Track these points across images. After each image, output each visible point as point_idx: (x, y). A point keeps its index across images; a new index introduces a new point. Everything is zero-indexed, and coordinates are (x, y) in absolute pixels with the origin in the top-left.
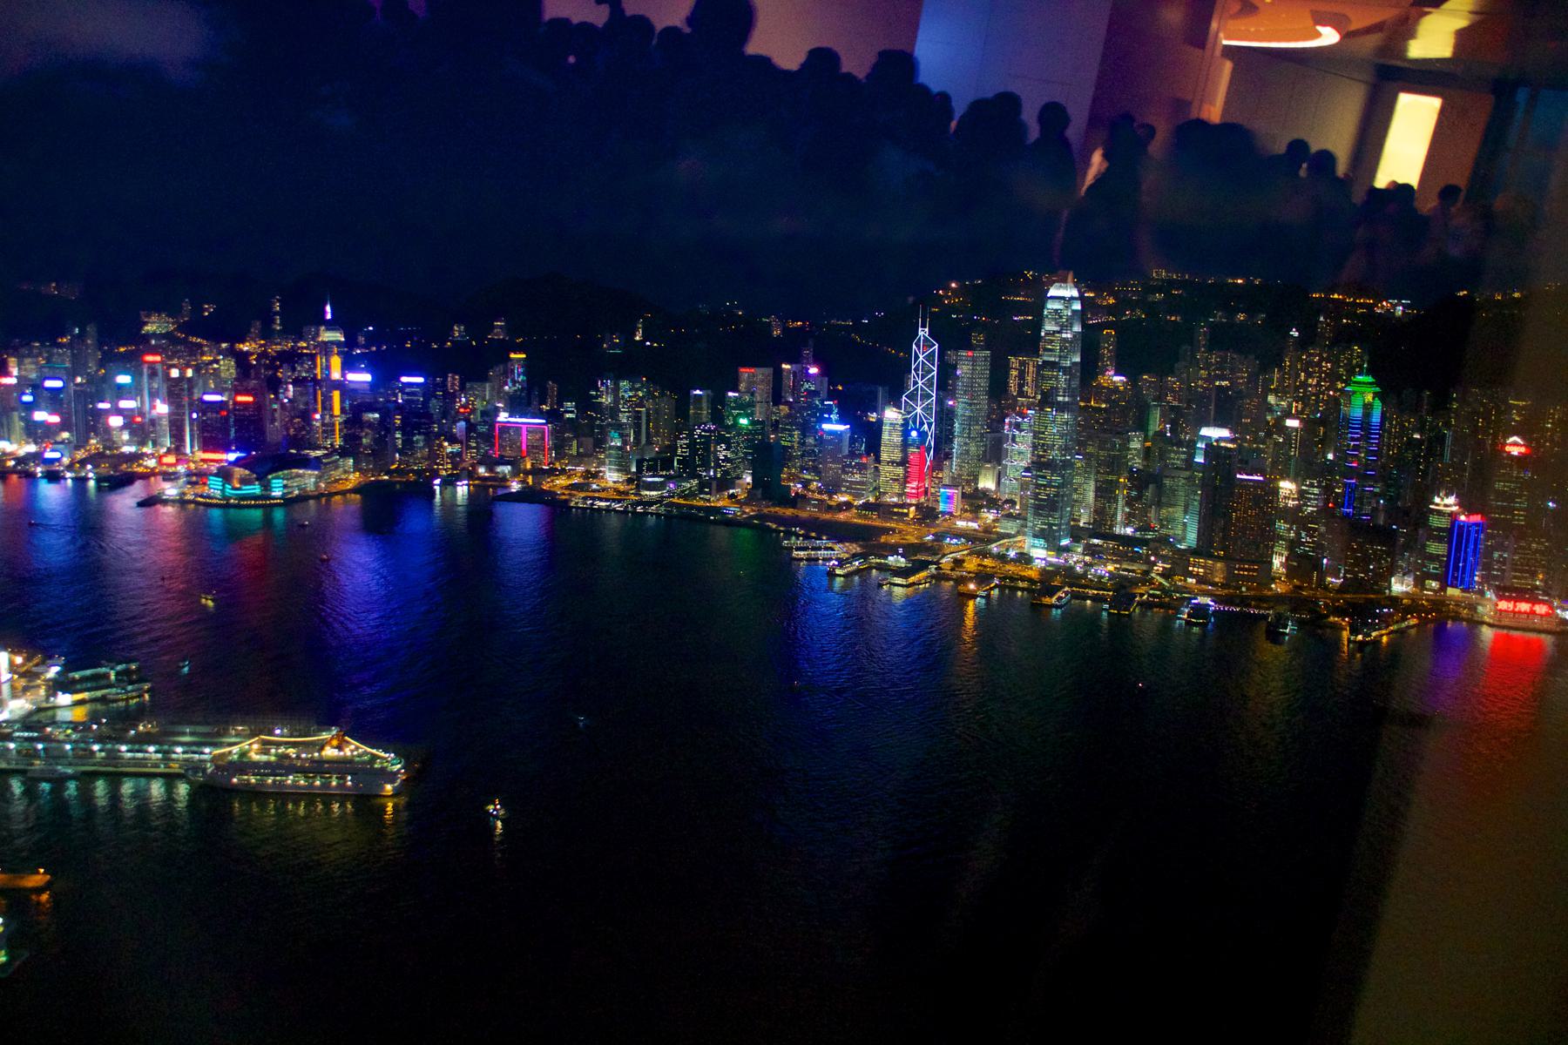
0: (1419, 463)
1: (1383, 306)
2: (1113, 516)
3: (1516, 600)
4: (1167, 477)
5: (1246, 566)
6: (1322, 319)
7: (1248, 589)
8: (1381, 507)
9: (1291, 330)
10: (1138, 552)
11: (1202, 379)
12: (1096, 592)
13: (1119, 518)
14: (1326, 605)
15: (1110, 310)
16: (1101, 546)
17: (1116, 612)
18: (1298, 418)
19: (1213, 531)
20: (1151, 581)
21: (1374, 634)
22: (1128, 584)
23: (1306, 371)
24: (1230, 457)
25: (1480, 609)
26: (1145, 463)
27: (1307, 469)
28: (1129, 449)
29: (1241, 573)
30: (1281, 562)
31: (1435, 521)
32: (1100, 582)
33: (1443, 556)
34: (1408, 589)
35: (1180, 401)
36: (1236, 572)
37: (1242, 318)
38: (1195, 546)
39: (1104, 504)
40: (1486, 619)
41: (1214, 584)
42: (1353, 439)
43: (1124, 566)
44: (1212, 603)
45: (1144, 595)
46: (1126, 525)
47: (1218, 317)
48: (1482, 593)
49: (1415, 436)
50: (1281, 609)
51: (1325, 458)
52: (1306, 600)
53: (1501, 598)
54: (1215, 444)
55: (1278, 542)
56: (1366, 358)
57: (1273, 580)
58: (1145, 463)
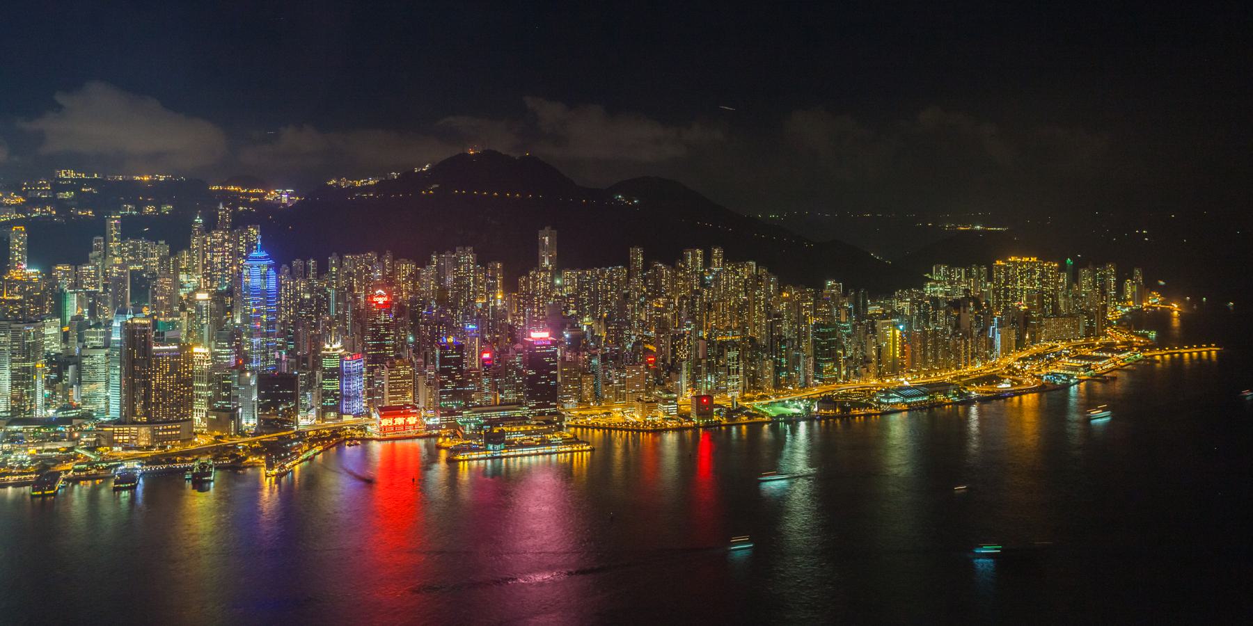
0: (312, 318)
1: (271, 195)
2: (31, 402)
3: (395, 416)
4: (87, 357)
5: (170, 427)
6: (221, 207)
7: (173, 446)
8: (284, 359)
9: (196, 218)
10: (61, 431)
11: (116, 265)
12: (17, 477)
13: (40, 400)
14: (245, 449)
15: (19, 209)
16: (21, 432)
17: (40, 493)
18: (208, 291)
19: (135, 400)
20: (75, 457)
21: (287, 465)
22: (52, 464)
23: (211, 251)
24: (145, 331)
25: (369, 428)
26: (64, 346)
27: (224, 333)
28: (44, 335)
29: (165, 433)
30: (202, 418)
31: (328, 364)
32: (21, 467)
33: (337, 390)
34: (313, 422)
35: (97, 287)
36: (160, 433)
37: (151, 210)
38: (119, 417)
39: (23, 390)
40: (375, 436)
41: (140, 448)
42: (255, 305)
43: (46, 448)
44: (140, 466)
45: (69, 471)
46: (47, 406)
47: (129, 209)
48: (369, 415)
49: (306, 297)
50: (203, 459)
51: (233, 322)
52: (226, 448)
53: (382, 416)
54: (130, 322)
55: (197, 401)
56: (259, 237)
57: (195, 434)
58: (64, 346)
